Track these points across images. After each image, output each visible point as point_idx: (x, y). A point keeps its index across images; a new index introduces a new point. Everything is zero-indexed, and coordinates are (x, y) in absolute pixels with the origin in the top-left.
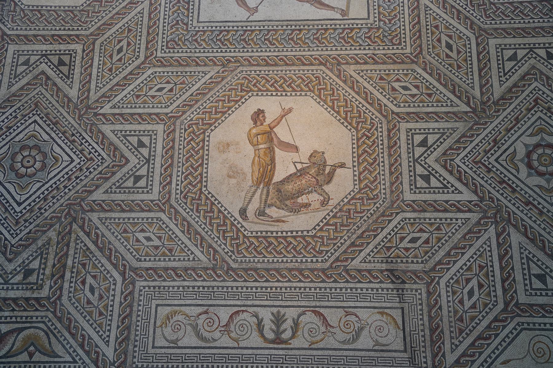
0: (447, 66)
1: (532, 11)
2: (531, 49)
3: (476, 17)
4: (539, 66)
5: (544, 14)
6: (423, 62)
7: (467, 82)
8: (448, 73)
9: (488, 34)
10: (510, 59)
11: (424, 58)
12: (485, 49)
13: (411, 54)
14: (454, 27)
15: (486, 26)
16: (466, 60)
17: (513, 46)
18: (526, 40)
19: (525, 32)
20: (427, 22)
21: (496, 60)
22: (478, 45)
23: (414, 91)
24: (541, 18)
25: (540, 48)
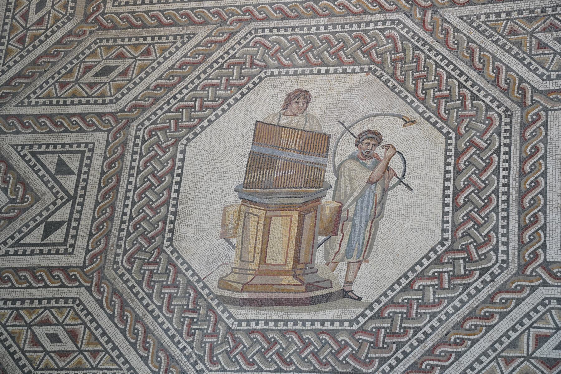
0: (69, 67)
1: (147, 205)
2: (73, 198)
3: (155, 114)
4: (38, 207)
5: (138, 223)
6: (84, 32)
7: (33, 97)
8: (56, 69)
9: (118, 131)
10: (61, 164)
11: (91, 32)
12: (88, 125)
13: (103, 14)
14: (142, 79)
15: (133, 130)
16: (74, 95)
17: (85, 169)
18: (92, 191)
19: (109, 190)
20: (160, 37)
21: (64, 141)
22: (100, 115)
23: (33, 18)
24: (131, 219)
25: (71, 213)
